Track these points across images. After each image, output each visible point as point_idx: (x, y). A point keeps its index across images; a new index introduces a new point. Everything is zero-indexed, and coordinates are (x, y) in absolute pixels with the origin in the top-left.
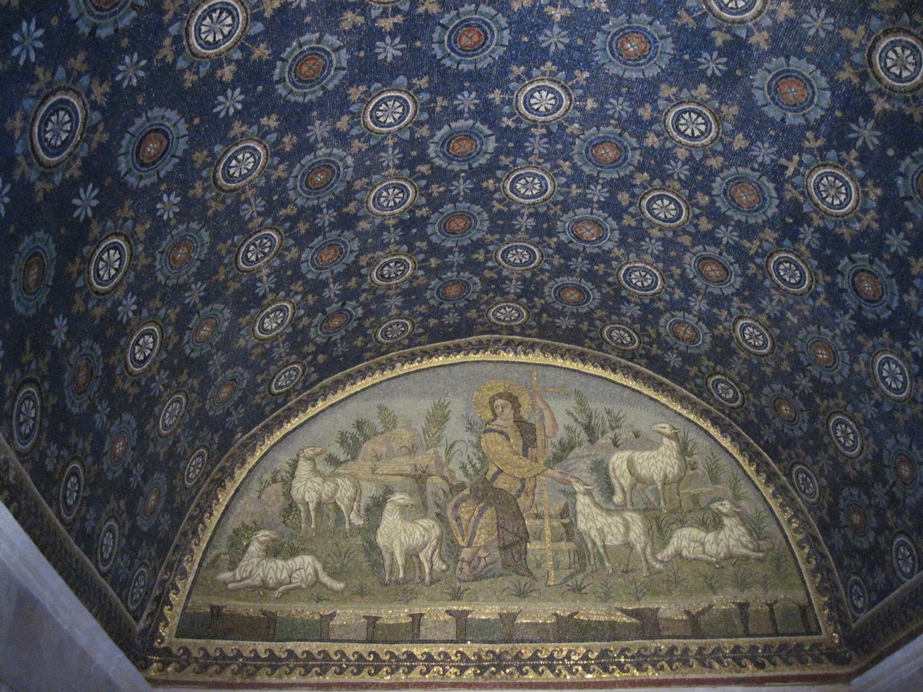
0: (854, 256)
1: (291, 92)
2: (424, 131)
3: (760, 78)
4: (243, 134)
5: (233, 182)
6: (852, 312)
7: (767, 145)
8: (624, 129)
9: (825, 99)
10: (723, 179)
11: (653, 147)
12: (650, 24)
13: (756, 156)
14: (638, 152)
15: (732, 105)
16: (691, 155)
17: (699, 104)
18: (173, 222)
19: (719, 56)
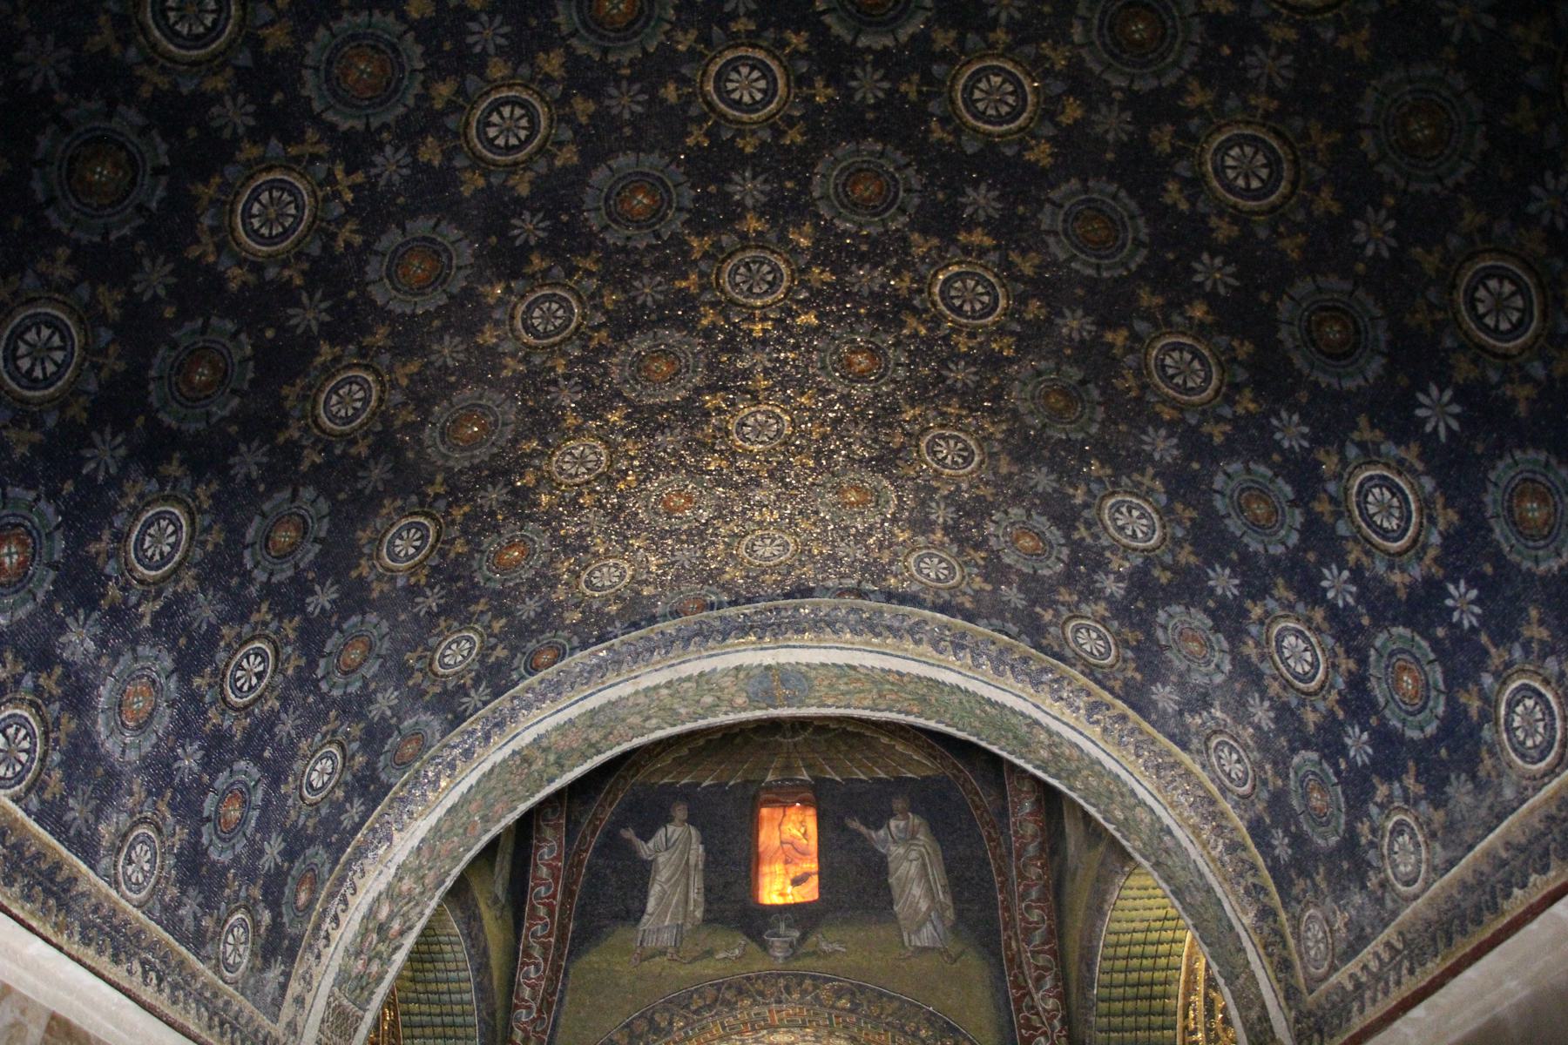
0: (164, 180)
1: (1132, 217)
2: (943, 39)
3: (465, 253)
4: (1220, 215)
5: (1273, 150)
6: (61, 97)
7: (396, 178)
8: (603, 63)
9: (378, 294)
10: (414, 71)
11: (547, 52)
12: (628, 238)
13: (397, 149)
14: (565, 30)
15: (473, 196)
16: (481, 75)
17: (516, 164)
18: (1390, 201)
19: (526, 241)
